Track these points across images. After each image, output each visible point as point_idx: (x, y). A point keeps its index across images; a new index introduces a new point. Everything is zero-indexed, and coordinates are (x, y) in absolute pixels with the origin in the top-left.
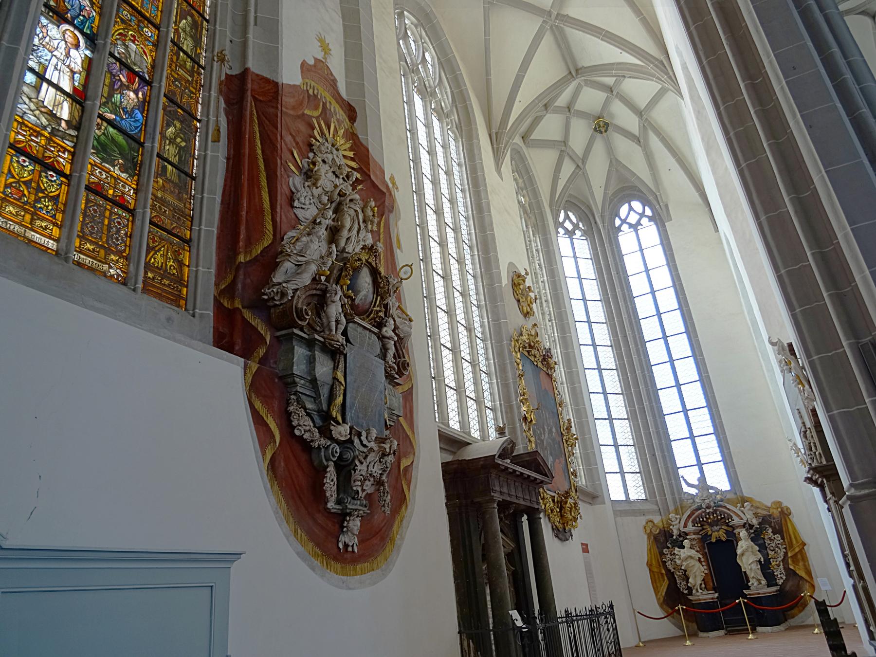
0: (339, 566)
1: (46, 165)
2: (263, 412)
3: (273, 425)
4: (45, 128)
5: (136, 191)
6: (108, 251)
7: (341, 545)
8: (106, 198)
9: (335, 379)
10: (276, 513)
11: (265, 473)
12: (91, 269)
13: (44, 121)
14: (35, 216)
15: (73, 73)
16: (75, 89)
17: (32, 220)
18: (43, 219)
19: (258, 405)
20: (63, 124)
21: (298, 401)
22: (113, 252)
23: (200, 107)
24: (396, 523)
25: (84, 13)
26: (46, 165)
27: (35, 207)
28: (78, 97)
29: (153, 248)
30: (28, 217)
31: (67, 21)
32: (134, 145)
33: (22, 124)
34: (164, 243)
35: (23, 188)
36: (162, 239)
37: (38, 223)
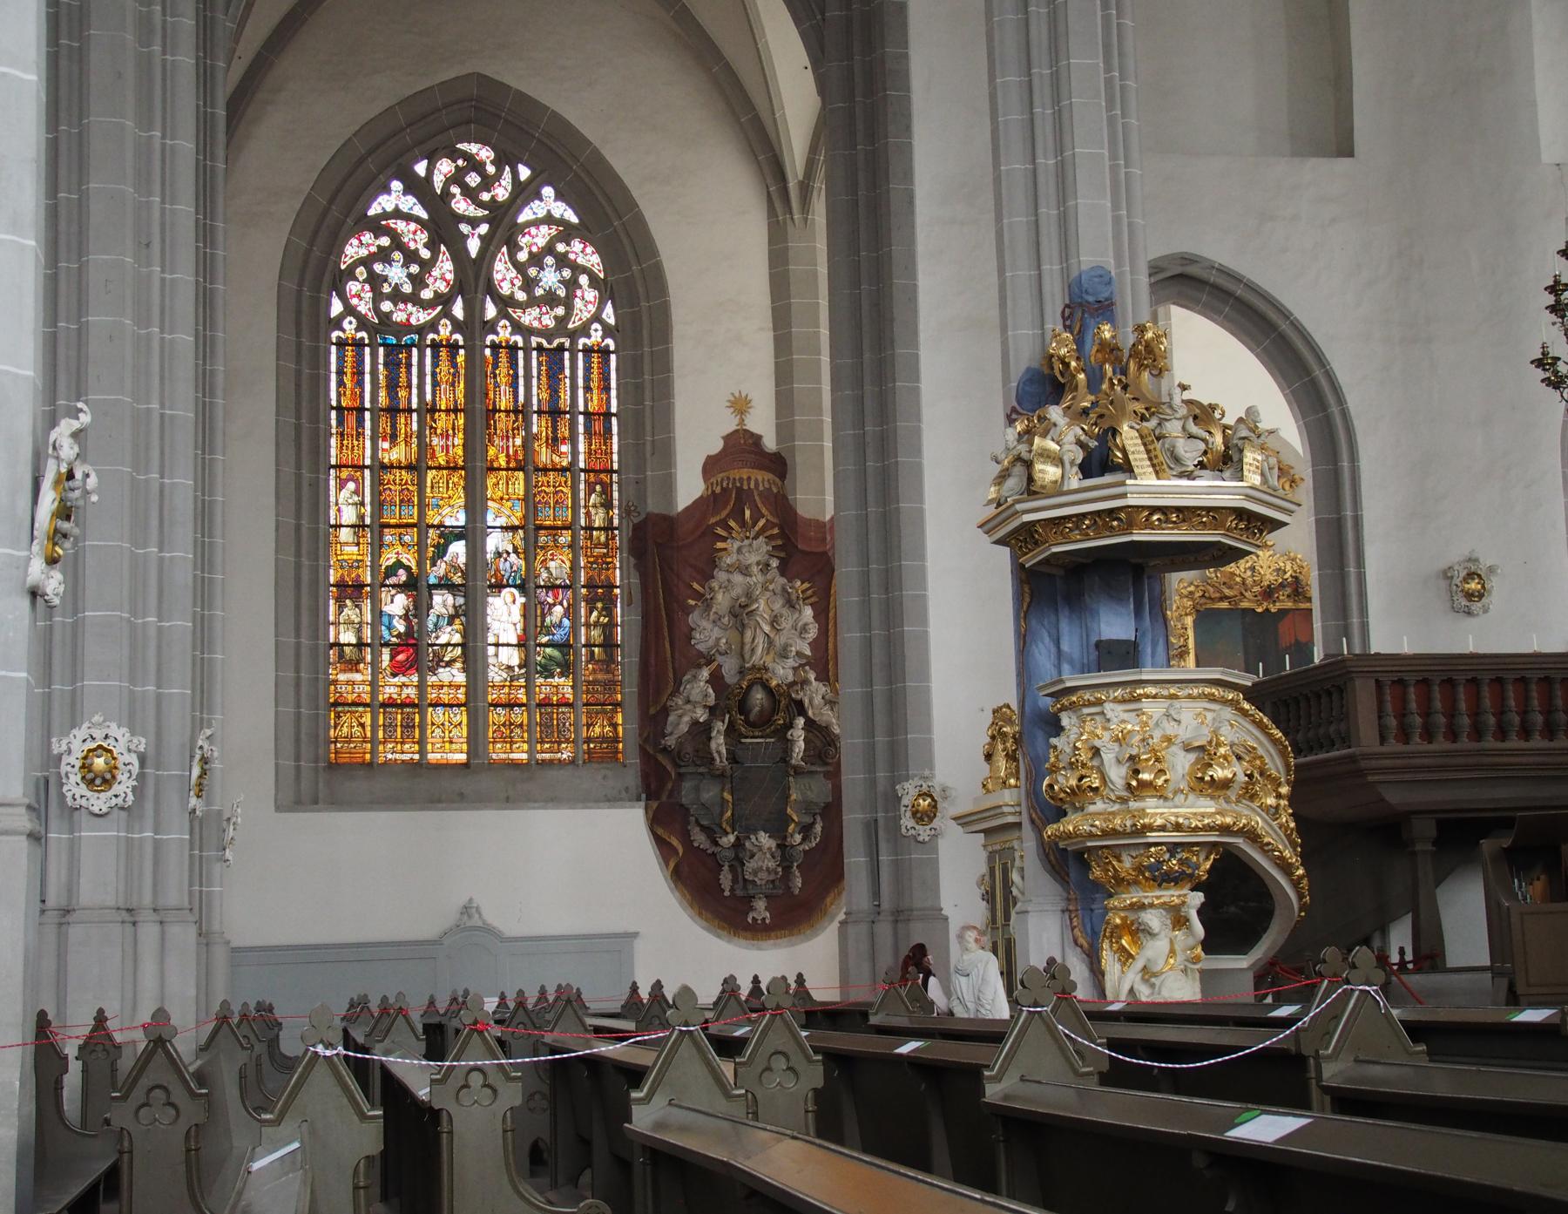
0: (749, 934)
1: (510, 705)
2: (665, 836)
3: (675, 842)
4: (506, 680)
5: (573, 687)
6: (559, 743)
7: (750, 920)
8: (552, 705)
9: (723, 798)
10: (680, 904)
11: (669, 878)
12: (551, 761)
13: (505, 675)
14: (512, 743)
15: (515, 624)
16: (518, 636)
17: (511, 746)
18: (516, 742)
19: (660, 831)
20: (516, 669)
21: (697, 821)
22: (563, 742)
23: (618, 571)
24: (832, 895)
25: (515, 568)
26: (510, 705)
27: (511, 737)
28: (522, 644)
29: (592, 724)
30: (508, 745)
31: (505, 587)
32: (565, 650)
33: (492, 687)
34: (599, 715)
35: (502, 728)
36: (597, 713)
37: (514, 746)
